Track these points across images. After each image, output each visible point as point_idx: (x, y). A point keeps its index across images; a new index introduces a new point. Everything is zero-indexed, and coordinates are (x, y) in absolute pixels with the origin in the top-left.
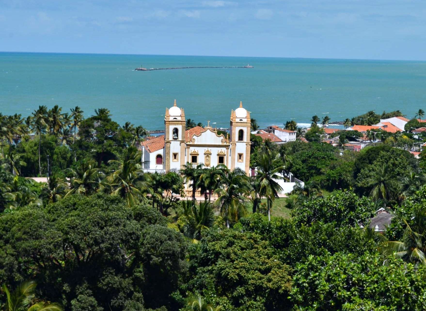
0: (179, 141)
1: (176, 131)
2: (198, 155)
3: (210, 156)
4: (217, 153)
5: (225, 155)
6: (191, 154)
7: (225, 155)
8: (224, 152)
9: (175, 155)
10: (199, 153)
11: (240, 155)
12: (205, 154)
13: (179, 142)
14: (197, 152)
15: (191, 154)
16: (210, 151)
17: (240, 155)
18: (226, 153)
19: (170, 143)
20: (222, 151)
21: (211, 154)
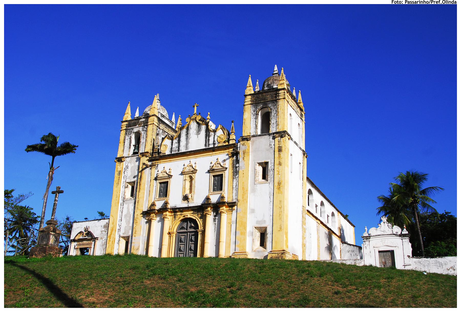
2: (170, 176)
6: (156, 179)
15: (156, 179)
18: (226, 166)
21: (194, 171)
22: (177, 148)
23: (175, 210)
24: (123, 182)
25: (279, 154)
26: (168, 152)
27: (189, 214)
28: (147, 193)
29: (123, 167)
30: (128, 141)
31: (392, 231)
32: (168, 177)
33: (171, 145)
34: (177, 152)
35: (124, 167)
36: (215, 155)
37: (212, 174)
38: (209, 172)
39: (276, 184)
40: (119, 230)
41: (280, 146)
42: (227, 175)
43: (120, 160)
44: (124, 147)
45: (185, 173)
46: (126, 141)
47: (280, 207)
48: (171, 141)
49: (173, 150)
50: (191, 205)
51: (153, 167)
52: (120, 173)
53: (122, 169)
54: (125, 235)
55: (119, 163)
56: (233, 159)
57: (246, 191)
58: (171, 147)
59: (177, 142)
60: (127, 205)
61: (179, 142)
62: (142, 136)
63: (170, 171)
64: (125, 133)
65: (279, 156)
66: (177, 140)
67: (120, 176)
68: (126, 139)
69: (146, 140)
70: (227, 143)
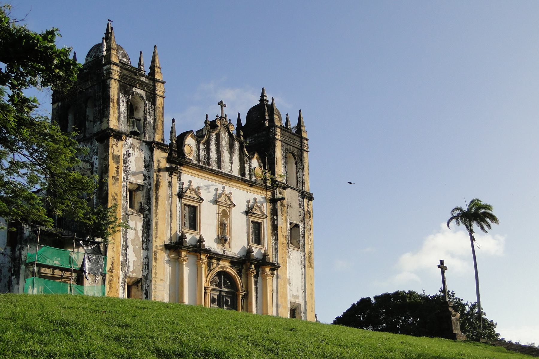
3: (228, 210)
6: (180, 195)
22: (206, 160)
24: (124, 178)
27: (226, 266)
28: (168, 215)
30: (124, 105)
32: (198, 200)
33: (197, 150)
34: (206, 166)
35: (124, 152)
36: (251, 192)
39: (307, 256)
40: (125, 263)
41: (309, 210)
45: (221, 204)
46: (121, 104)
49: (200, 159)
50: (229, 253)
54: (134, 274)
55: (115, 140)
58: (197, 152)
59: (205, 149)
60: (134, 222)
61: (208, 150)
66: (205, 146)
68: (121, 99)
69: (155, 120)
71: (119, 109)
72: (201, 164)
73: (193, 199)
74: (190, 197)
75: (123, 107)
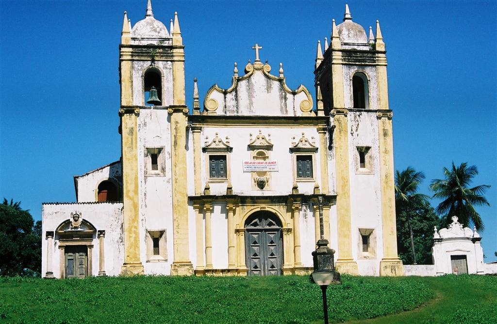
0: (167, 108)
1: (153, 80)
4: (292, 146)
5: (315, 150)
7: (315, 150)
8: (311, 141)
9: (154, 155)
10: (231, 146)
11: (363, 152)
12: (251, 147)
13: (165, 113)
14: (224, 141)
16: (267, 138)
17: (363, 152)
19: (138, 115)
20: (307, 137)
21: (269, 147)
23: (243, 200)
25: (385, 139)
26: (220, 112)
29: (136, 123)
31: (464, 233)
33: (224, 101)
37: (295, 155)
38: (292, 150)
41: (385, 128)
42: (317, 158)
43: (130, 110)
44: (132, 89)
47: (390, 206)
48: (222, 95)
51: (195, 131)
52: (131, 131)
53: (136, 125)
55: (128, 114)
56: (325, 137)
57: (347, 182)
58: (224, 104)
59: (234, 98)
62: (165, 78)
63: (227, 140)
64: (130, 66)
65: (385, 142)
66: (234, 95)
67: (134, 137)
68: (134, 76)
70: (313, 115)
71: (132, 85)
72: (228, 114)
73: (219, 150)
74: (214, 149)
75: (138, 83)
